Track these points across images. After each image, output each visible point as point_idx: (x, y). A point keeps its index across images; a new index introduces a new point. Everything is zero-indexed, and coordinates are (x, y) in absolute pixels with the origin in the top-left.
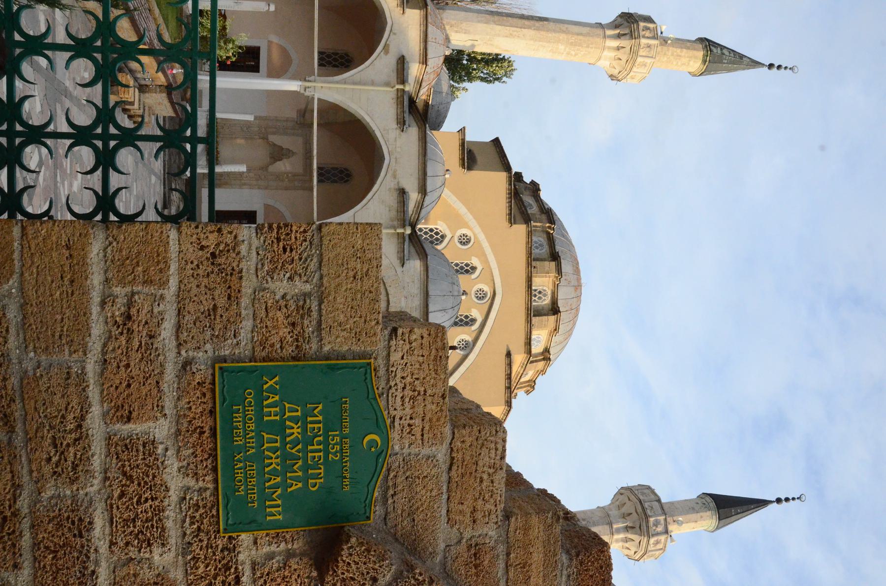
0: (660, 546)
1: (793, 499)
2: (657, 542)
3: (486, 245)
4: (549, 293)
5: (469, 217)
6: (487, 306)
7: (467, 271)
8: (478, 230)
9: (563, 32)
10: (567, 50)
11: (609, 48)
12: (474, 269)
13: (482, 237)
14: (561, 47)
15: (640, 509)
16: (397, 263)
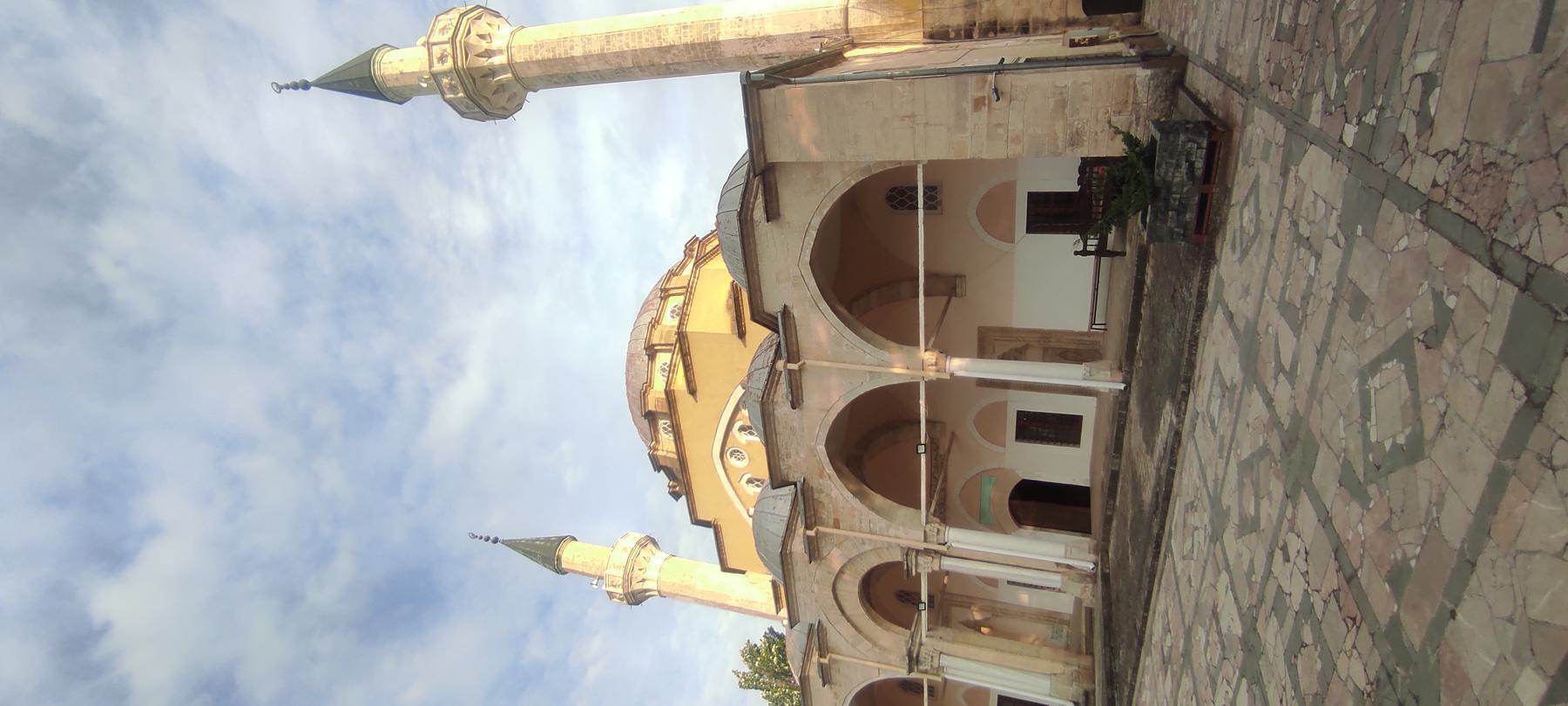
0: (437, 51)
4: (661, 431)
6: (729, 444)
15: (483, 103)
16: (826, 624)
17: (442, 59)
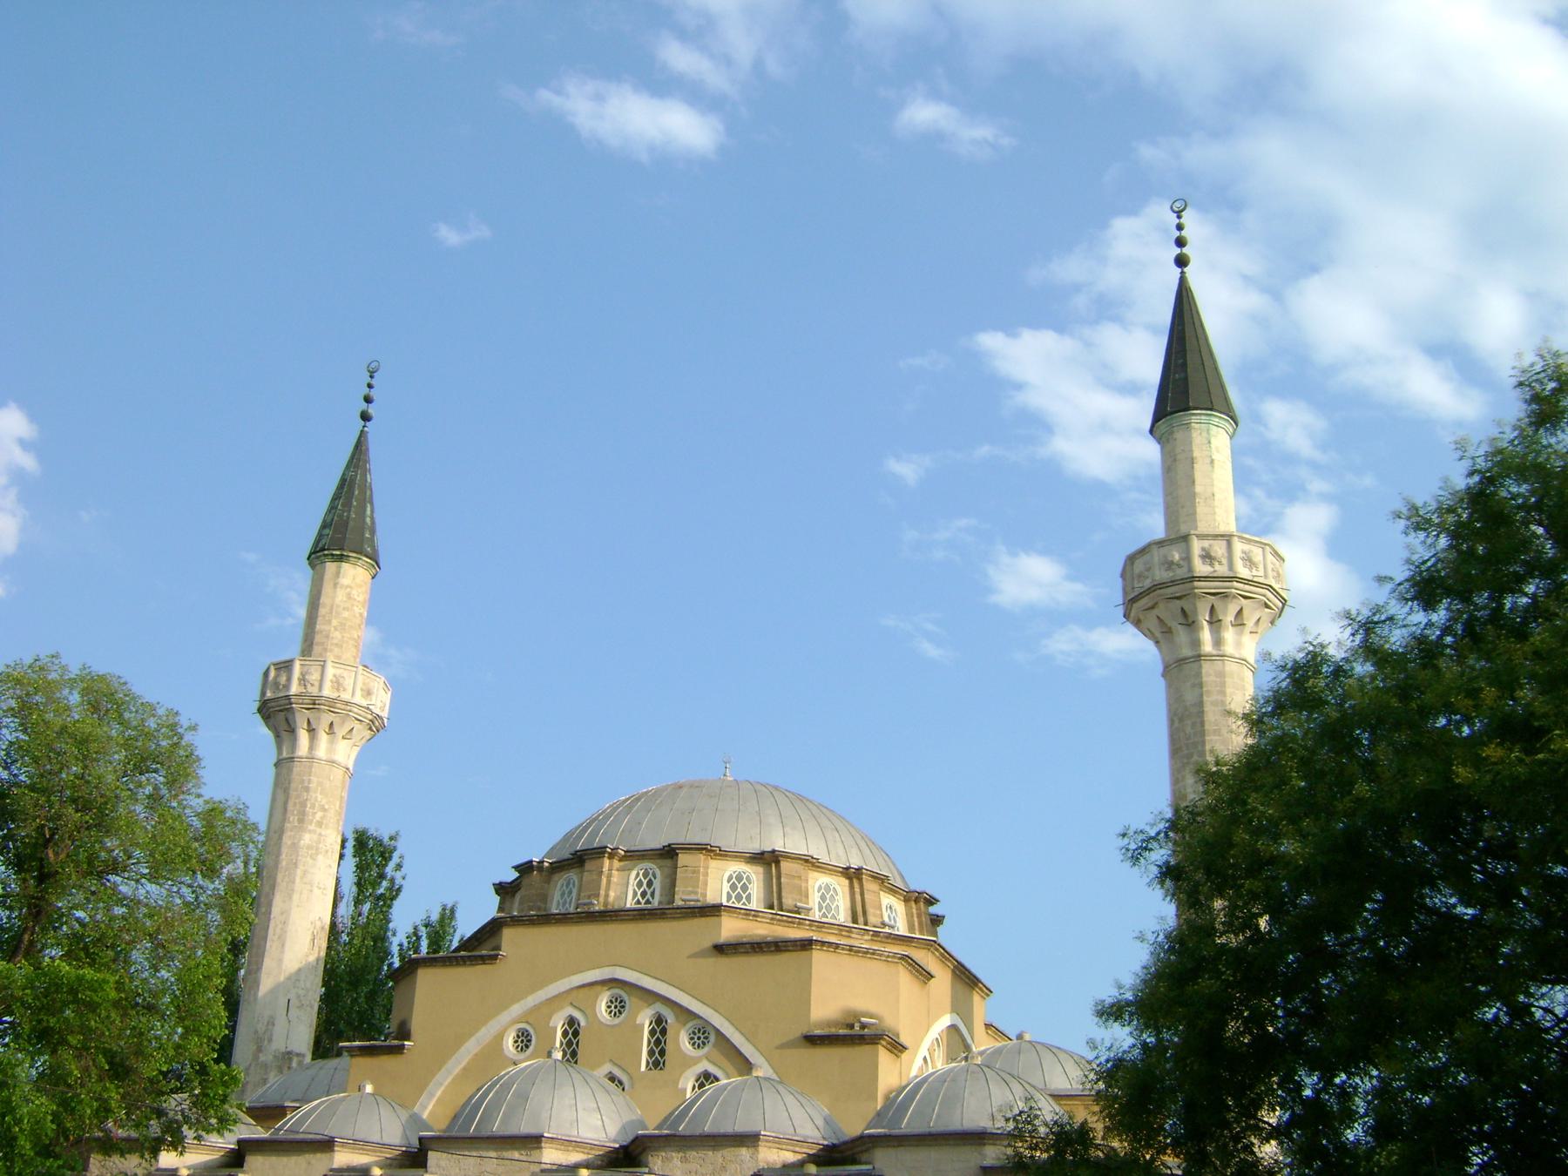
0: (1219, 549)
1: (1180, 227)
2: (1207, 557)
3: (531, 1000)
5: (485, 1034)
7: (576, 1034)
8: (505, 1017)
9: (280, 838)
10: (312, 827)
11: (311, 748)
12: (572, 1021)
13: (517, 1009)
14: (307, 839)
17: (1207, 557)
